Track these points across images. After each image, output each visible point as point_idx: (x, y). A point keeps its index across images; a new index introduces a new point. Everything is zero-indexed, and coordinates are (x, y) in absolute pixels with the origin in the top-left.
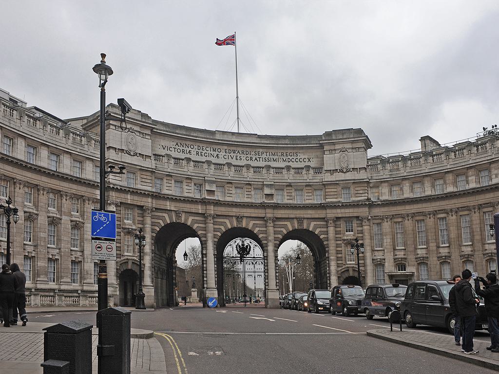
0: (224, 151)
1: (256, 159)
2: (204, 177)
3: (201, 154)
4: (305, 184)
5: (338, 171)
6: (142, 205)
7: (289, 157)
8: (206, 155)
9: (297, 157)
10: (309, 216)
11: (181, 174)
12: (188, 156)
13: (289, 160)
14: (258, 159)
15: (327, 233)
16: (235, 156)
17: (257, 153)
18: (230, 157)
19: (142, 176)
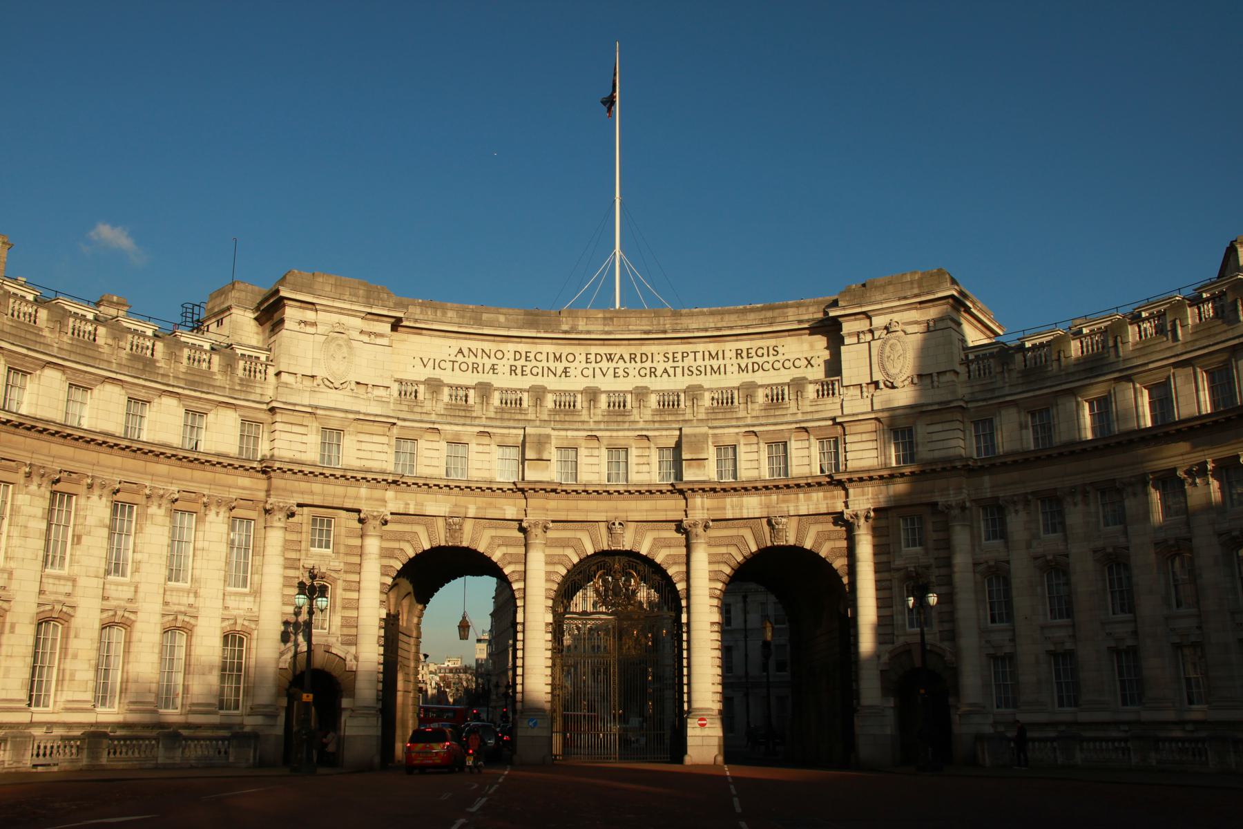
0: (583, 358)
1: (666, 371)
2: (525, 429)
3: (522, 371)
4: (794, 426)
5: (882, 385)
6: (356, 506)
7: (756, 359)
8: (535, 371)
9: (776, 358)
10: (803, 511)
11: (464, 425)
12: (487, 378)
13: (756, 367)
14: (671, 371)
16: (611, 371)
17: (670, 356)
18: (597, 371)
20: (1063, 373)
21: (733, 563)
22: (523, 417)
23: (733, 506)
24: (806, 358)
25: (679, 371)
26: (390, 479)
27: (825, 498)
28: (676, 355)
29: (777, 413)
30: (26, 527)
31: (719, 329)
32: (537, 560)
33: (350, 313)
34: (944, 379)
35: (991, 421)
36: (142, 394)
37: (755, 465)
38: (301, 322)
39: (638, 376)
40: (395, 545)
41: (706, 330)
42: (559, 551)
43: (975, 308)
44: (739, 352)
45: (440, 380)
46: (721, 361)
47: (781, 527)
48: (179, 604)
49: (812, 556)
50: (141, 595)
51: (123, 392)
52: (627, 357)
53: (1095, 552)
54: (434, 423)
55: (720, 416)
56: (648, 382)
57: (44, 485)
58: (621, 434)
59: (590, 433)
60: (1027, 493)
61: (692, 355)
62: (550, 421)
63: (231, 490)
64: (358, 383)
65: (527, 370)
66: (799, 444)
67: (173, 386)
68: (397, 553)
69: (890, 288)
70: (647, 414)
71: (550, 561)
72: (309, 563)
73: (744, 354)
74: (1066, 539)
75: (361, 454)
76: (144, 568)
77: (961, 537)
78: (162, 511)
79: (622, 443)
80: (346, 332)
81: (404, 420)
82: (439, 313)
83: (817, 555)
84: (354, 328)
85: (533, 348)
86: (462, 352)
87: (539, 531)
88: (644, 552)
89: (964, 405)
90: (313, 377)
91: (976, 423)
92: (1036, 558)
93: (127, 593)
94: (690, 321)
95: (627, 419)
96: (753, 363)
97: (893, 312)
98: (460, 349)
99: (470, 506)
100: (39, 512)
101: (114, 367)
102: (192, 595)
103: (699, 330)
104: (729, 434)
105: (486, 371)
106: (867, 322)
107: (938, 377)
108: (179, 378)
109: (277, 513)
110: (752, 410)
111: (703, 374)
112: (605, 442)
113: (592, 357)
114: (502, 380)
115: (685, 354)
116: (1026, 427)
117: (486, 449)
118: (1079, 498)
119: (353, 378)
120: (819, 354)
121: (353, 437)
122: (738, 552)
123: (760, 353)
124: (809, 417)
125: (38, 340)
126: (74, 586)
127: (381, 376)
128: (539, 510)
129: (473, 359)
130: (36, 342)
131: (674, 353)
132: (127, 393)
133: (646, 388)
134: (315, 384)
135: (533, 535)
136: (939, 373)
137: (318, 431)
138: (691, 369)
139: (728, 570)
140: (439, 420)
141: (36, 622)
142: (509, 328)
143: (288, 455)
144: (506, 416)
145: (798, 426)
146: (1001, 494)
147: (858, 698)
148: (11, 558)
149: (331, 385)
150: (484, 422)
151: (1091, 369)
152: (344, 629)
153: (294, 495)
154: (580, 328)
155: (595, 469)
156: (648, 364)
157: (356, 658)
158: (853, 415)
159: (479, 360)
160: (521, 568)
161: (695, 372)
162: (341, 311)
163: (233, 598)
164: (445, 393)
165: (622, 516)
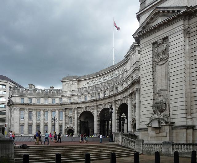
0: (103, 78)
36: (46, 98)
42: (99, 109)
64: (72, 91)
71: (97, 111)
72: (69, 115)
79: (105, 90)
100: (35, 114)
112: (103, 91)
143: (64, 102)
155: (102, 96)
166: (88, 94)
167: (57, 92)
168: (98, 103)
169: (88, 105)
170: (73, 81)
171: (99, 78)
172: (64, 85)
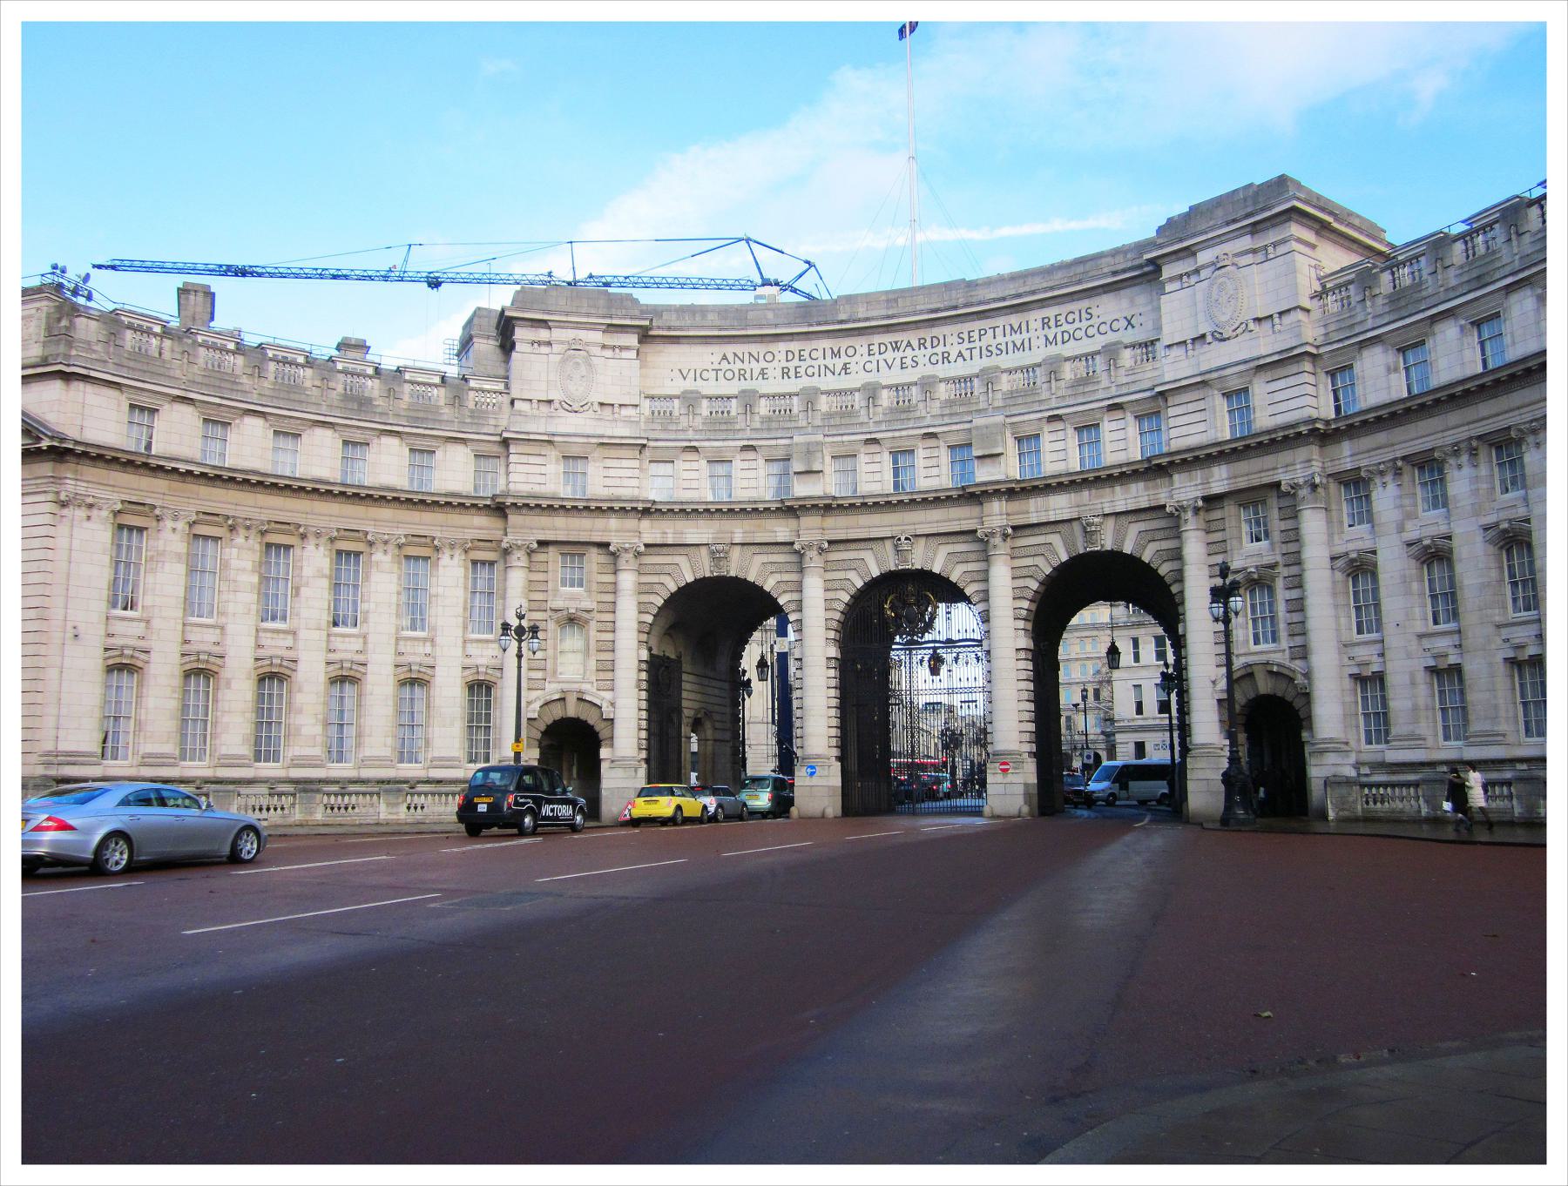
0: (865, 350)
1: (960, 354)
3: (796, 373)
5: (1209, 339)
6: (605, 539)
7: (1066, 327)
8: (810, 372)
9: (1089, 323)
13: (1066, 336)
14: (967, 354)
15: (1177, 555)
16: (898, 362)
17: (965, 336)
18: (882, 364)
19: (609, 463)
20: (1442, 289)
21: (1041, 577)
22: (793, 424)
23: (1037, 509)
24: (1126, 318)
25: (976, 352)
26: (640, 506)
27: (1146, 488)
28: (971, 334)
29: (1086, 390)
30: (235, 581)
31: (1019, 296)
32: (814, 587)
33: (588, 326)
34: (1287, 319)
35: (1351, 367)
36: (358, 436)
37: (1061, 455)
38: (533, 343)
39: (928, 365)
40: (654, 579)
41: (1004, 299)
43: (1342, 223)
44: (1046, 321)
45: (698, 392)
46: (1025, 335)
47: (1093, 529)
48: (415, 654)
49: (1133, 561)
50: (370, 646)
51: (337, 435)
52: (915, 343)
53: (1486, 529)
54: (690, 440)
55: (1020, 401)
56: (943, 371)
57: (252, 537)
58: (904, 433)
59: (869, 436)
60: (1396, 459)
61: (990, 332)
62: (824, 426)
63: (466, 530)
64: (602, 404)
65: (802, 370)
66: (1114, 425)
67: (391, 424)
68: (657, 588)
69: (1220, 212)
70: (935, 407)
72: (559, 604)
73: (1052, 323)
74: (1448, 517)
75: (609, 482)
76: (372, 618)
77: (1313, 524)
78: (388, 558)
79: (906, 445)
80: (587, 348)
81: (657, 440)
82: (698, 318)
83: (1140, 559)
84: (595, 344)
85: (808, 346)
86: (726, 359)
87: (813, 553)
88: (936, 570)
89: (1314, 351)
90: (550, 402)
91: (1332, 374)
92: (1409, 545)
93: (357, 644)
94: (986, 291)
95: (911, 415)
96: (1063, 332)
97: (1222, 242)
98: (725, 355)
99: (736, 530)
100: (249, 565)
101: (324, 410)
102: (428, 644)
103: (995, 300)
104: (1030, 420)
105: (755, 376)
106: (1190, 260)
107: (1280, 318)
108: (399, 415)
109: (515, 552)
110: (1058, 388)
111: (1004, 352)
112: (888, 444)
113: (875, 348)
114: (775, 384)
115: (983, 332)
116: (1396, 370)
117: (753, 464)
118: (1465, 458)
119: (596, 398)
120: (1141, 310)
121: (597, 464)
122: (1046, 563)
123: (1070, 319)
124: (1125, 390)
125: (235, 387)
126: (295, 640)
127: (629, 393)
128: (812, 529)
129: (739, 365)
130: (232, 390)
131: (969, 332)
132: (341, 436)
133: (934, 376)
134: (552, 410)
135: (807, 558)
136: (1281, 314)
137: (557, 461)
138: (990, 348)
139: (1034, 585)
140: (696, 437)
141: (254, 677)
142: (776, 326)
143: (524, 488)
144: (774, 425)
145: (1111, 402)
146: (1363, 463)
147: (1190, 736)
148: (223, 614)
149: (570, 409)
150: (748, 434)
151: (1479, 277)
152: (601, 673)
153: (534, 531)
154: (860, 316)
155: (877, 477)
156: (940, 349)
157: (613, 704)
158: (1175, 381)
159: (746, 366)
160: (795, 596)
161: (995, 351)
162: (578, 326)
163: (474, 645)
164: (705, 408)
165: (910, 530)
166: (745, 448)
167: (457, 399)
168: (840, 526)
169: (739, 530)
170: (612, 328)
171: (826, 344)
172: (527, 348)
